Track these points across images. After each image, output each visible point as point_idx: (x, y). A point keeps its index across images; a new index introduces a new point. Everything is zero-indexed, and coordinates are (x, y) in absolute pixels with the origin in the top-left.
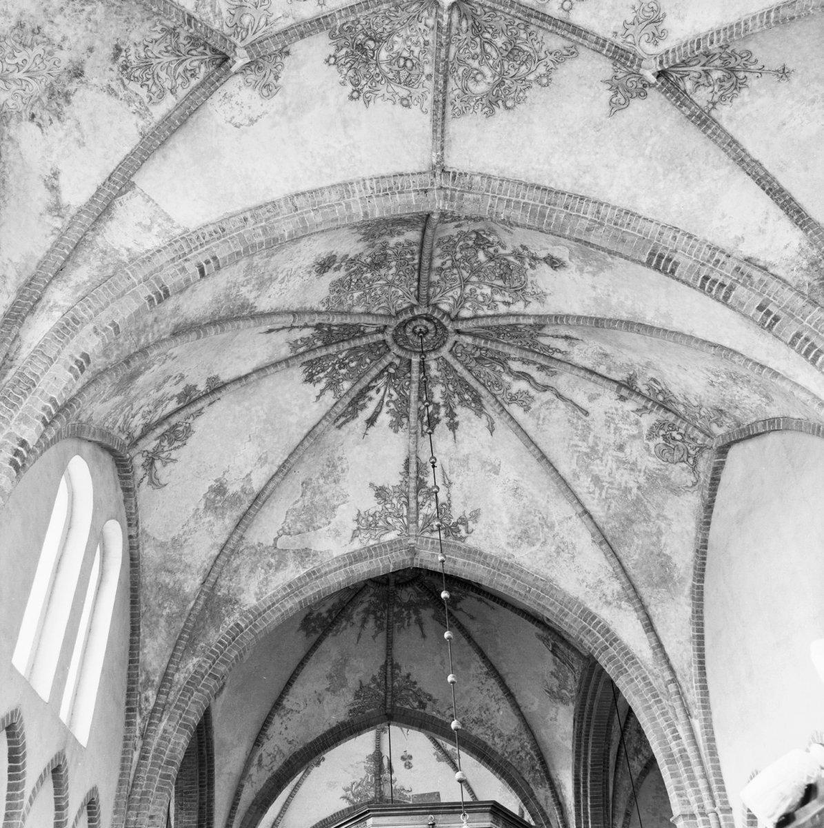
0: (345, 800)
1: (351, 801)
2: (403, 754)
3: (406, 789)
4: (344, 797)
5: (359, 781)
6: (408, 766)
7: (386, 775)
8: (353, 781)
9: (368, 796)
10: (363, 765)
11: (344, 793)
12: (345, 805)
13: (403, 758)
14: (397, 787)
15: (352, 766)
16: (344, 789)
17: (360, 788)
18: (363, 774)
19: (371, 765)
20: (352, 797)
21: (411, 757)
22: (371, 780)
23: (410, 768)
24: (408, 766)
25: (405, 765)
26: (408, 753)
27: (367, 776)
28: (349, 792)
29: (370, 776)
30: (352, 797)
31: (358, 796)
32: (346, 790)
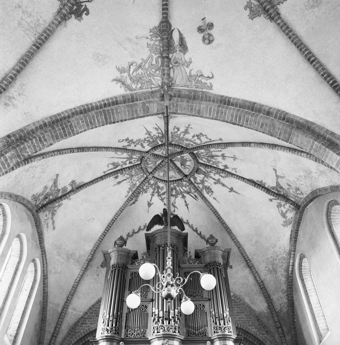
0: (119, 84)
1: (128, 87)
2: (200, 23)
3: (206, 75)
4: (117, 80)
5: (139, 62)
6: (208, 40)
7: (176, 55)
8: (130, 60)
9: (152, 83)
10: (145, 42)
11: (118, 75)
12: (119, 91)
13: (200, 30)
14: (193, 73)
15: (129, 39)
16: (118, 69)
17: (140, 71)
18: (145, 53)
19: (156, 42)
20: (129, 82)
21: (211, 26)
22: (157, 62)
23: (210, 42)
24: (208, 40)
25: (204, 39)
26: (208, 21)
27: (150, 57)
28: (126, 74)
29: (155, 57)
30: (129, 82)
31: (138, 81)
32: (122, 71)
